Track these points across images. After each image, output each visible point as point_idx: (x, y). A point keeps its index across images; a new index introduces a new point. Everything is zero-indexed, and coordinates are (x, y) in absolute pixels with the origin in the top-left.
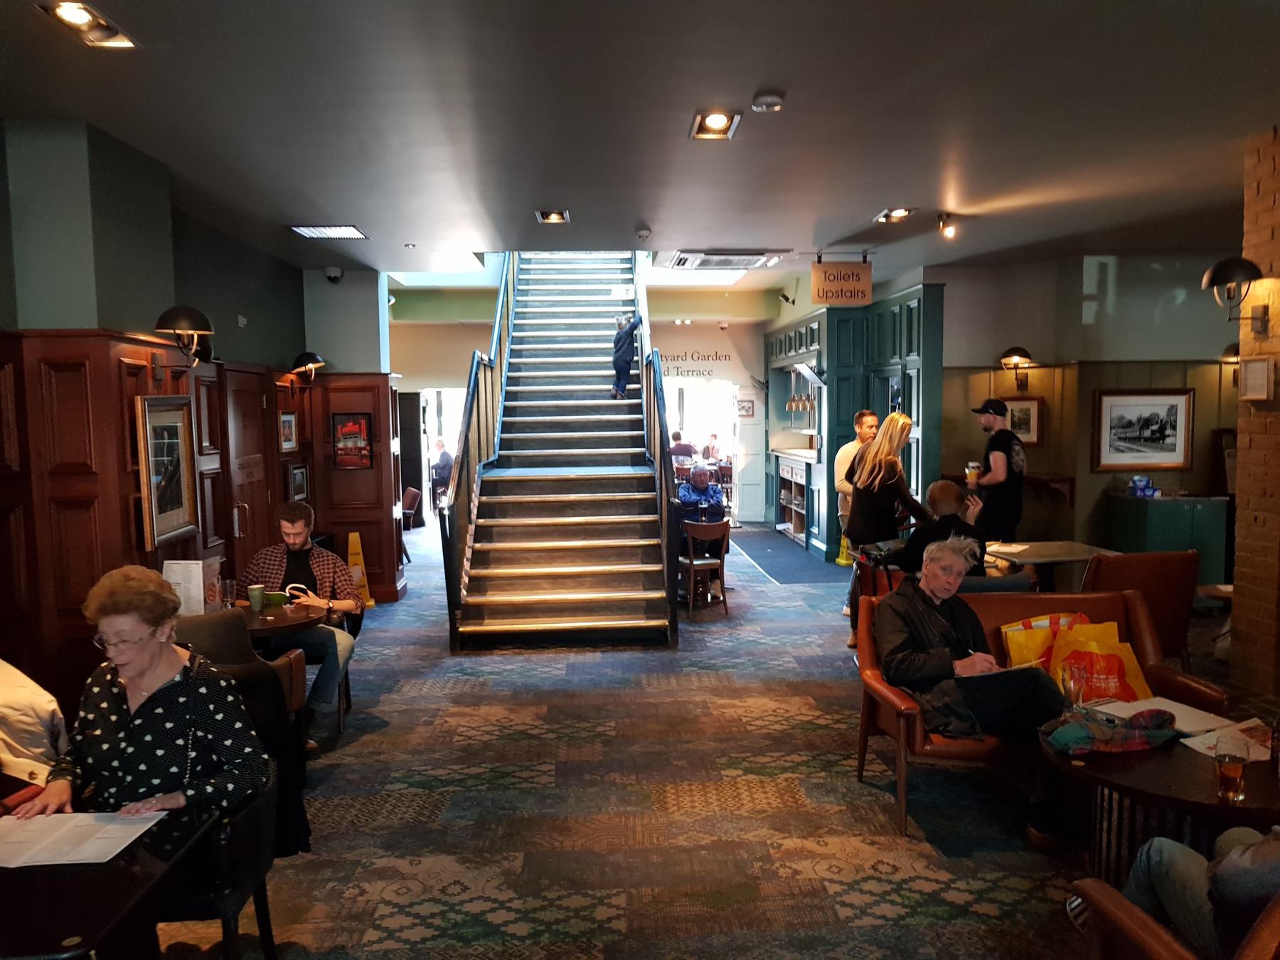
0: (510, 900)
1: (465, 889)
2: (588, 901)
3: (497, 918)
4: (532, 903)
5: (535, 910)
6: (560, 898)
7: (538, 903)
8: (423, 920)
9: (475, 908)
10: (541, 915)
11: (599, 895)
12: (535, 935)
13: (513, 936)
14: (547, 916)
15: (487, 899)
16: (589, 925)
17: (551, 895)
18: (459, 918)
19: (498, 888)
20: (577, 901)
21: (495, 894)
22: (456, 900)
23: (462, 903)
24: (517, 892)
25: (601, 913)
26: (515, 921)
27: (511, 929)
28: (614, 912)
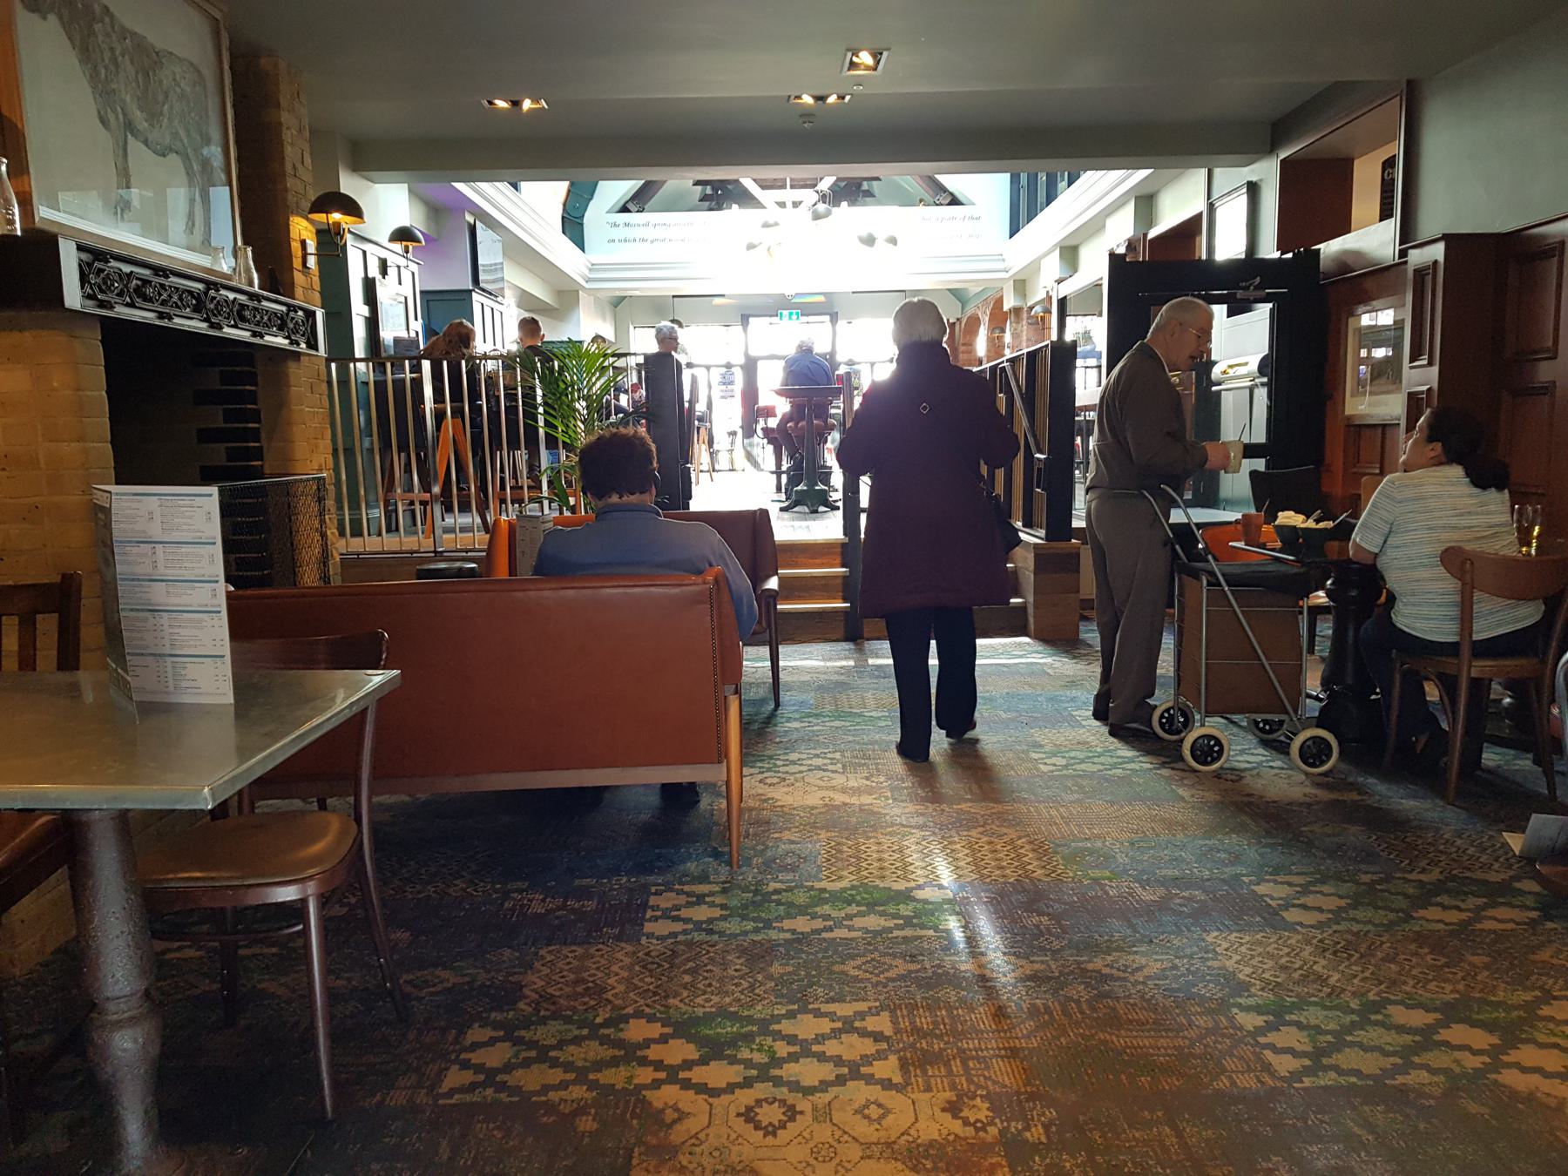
0: (657, 1084)
1: (749, 1115)
3: (680, 1051)
4: (614, 1077)
5: (614, 1062)
6: (564, 1085)
7: (607, 1077)
8: (805, 1050)
9: (717, 1073)
11: (489, 1092)
12: (618, 1020)
13: (651, 1019)
15: (702, 1089)
17: (578, 1092)
18: (745, 1054)
19: (682, 1116)
21: (687, 1099)
22: (762, 1090)
23: (747, 1083)
24: (645, 1102)
26: (647, 1043)
27: (656, 1030)
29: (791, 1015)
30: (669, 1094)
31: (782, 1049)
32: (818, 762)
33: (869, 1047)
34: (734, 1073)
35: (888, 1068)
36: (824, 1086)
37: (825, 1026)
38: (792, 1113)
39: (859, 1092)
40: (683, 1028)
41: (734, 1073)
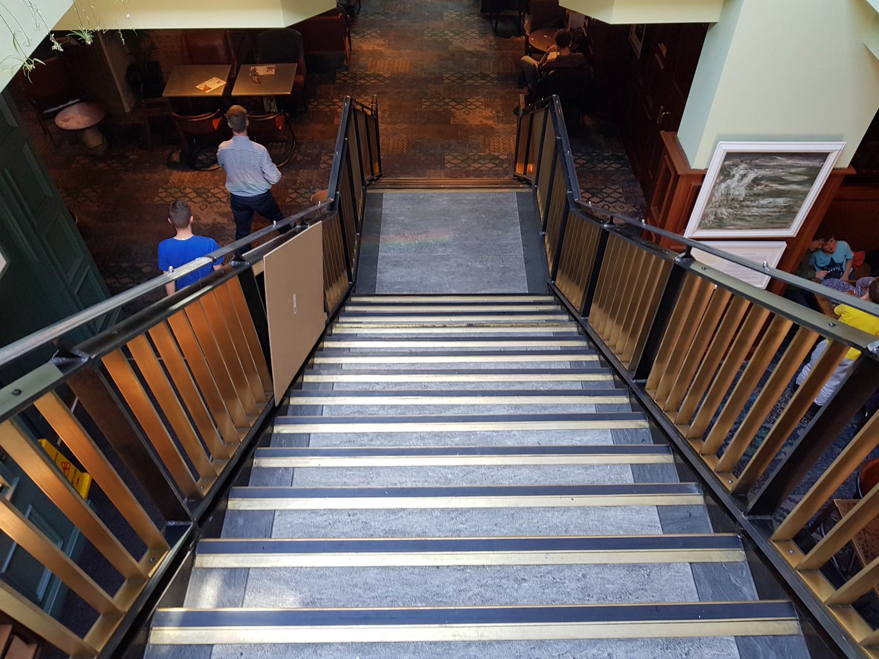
1: (464, 112)
2: (433, 107)
3: (454, 103)
4: (446, 107)
8: (471, 104)
9: (459, 107)
10: (442, 104)
12: (444, 99)
14: (441, 103)
15: (457, 109)
16: (431, 100)
18: (463, 104)
20: (434, 107)
22: (466, 109)
23: (463, 108)
25: (428, 103)
27: (450, 100)
28: (425, 104)
29: (469, 98)
30: (453, 110)
31: (468, 103)
32: (474, 35)
33: (481, 103)
34: (462, 107)
35: (483, 107)
36: (474, 109)
37: (474, 100)
38: (470, 112)
39: (479, 110)
40: (454, 100)
41: (462, 107)
